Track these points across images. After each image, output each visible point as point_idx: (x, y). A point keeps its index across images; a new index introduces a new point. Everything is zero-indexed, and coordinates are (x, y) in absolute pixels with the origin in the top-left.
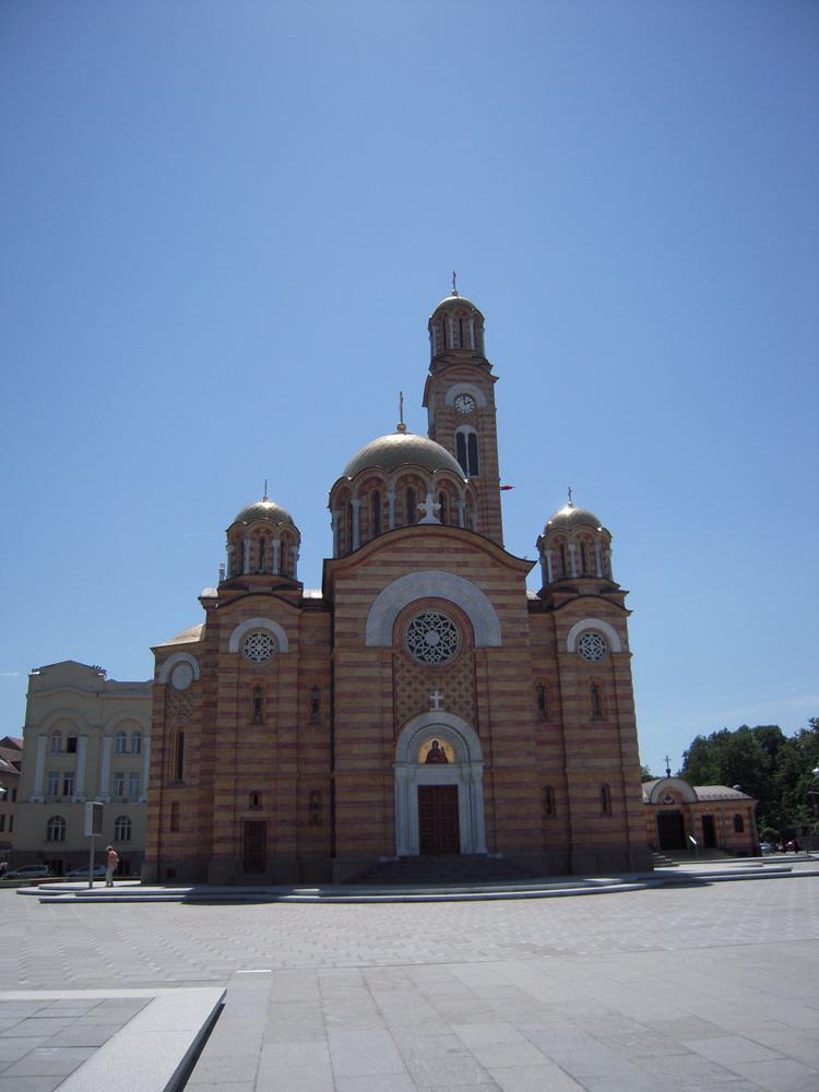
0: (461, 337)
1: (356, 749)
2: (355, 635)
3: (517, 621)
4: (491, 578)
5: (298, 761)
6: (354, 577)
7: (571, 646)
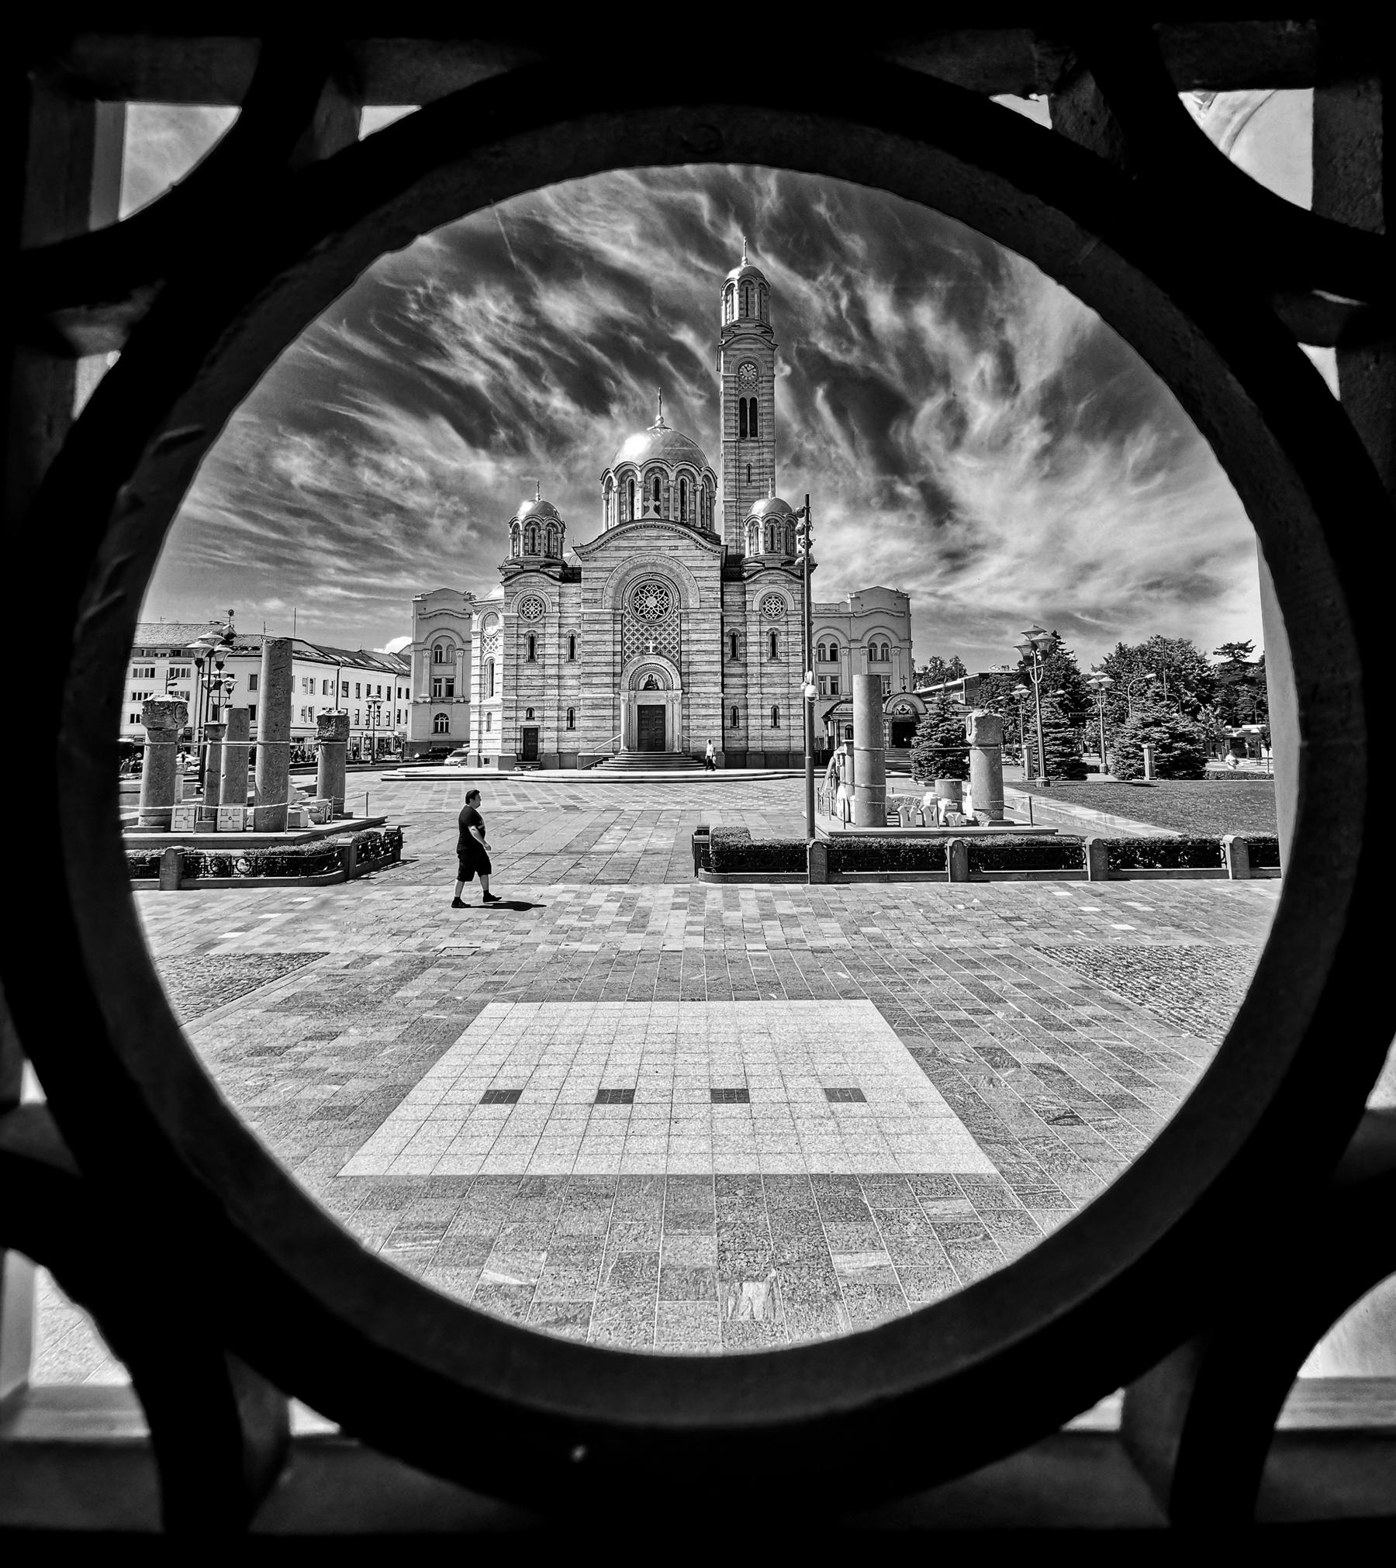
3: (711, 589)
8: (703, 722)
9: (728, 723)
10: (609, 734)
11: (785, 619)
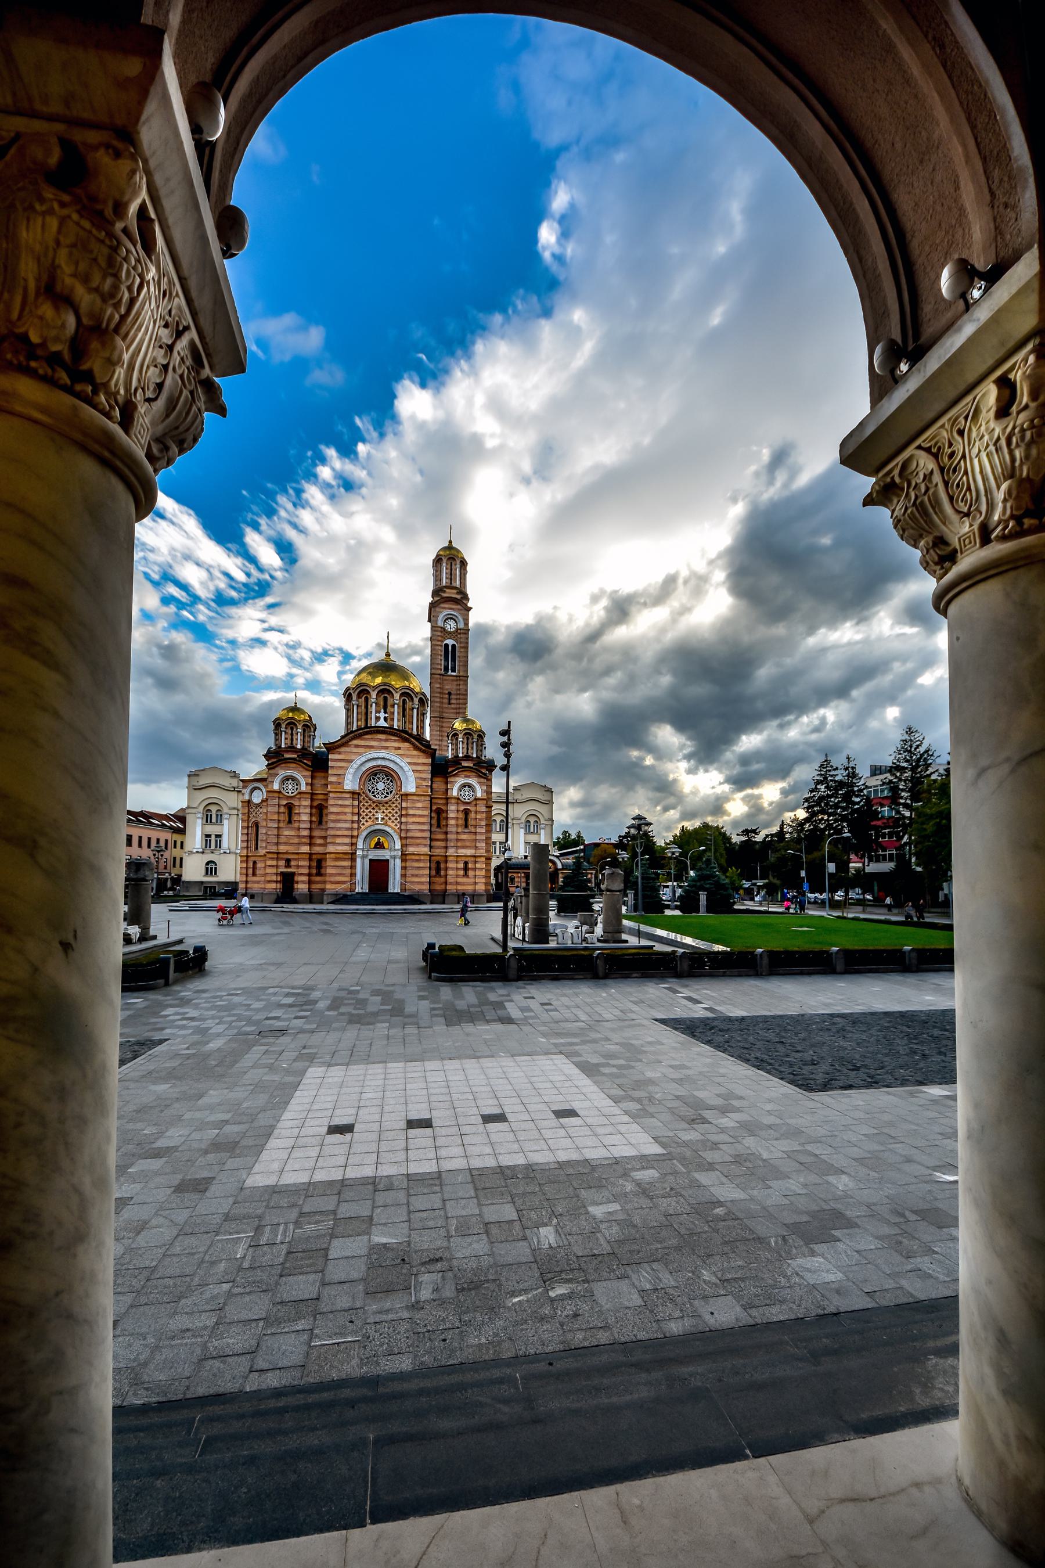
0: (451, 578)
1: (338, 840)
2: (339, 783)
3: (424, 779)
4: (412, 756)
5: (311, 844)
6: (340, 753)
7: (455, 793)
8: (416, 872)
9: (433, 873)
10: (347, 879)
11: (474, 803)
